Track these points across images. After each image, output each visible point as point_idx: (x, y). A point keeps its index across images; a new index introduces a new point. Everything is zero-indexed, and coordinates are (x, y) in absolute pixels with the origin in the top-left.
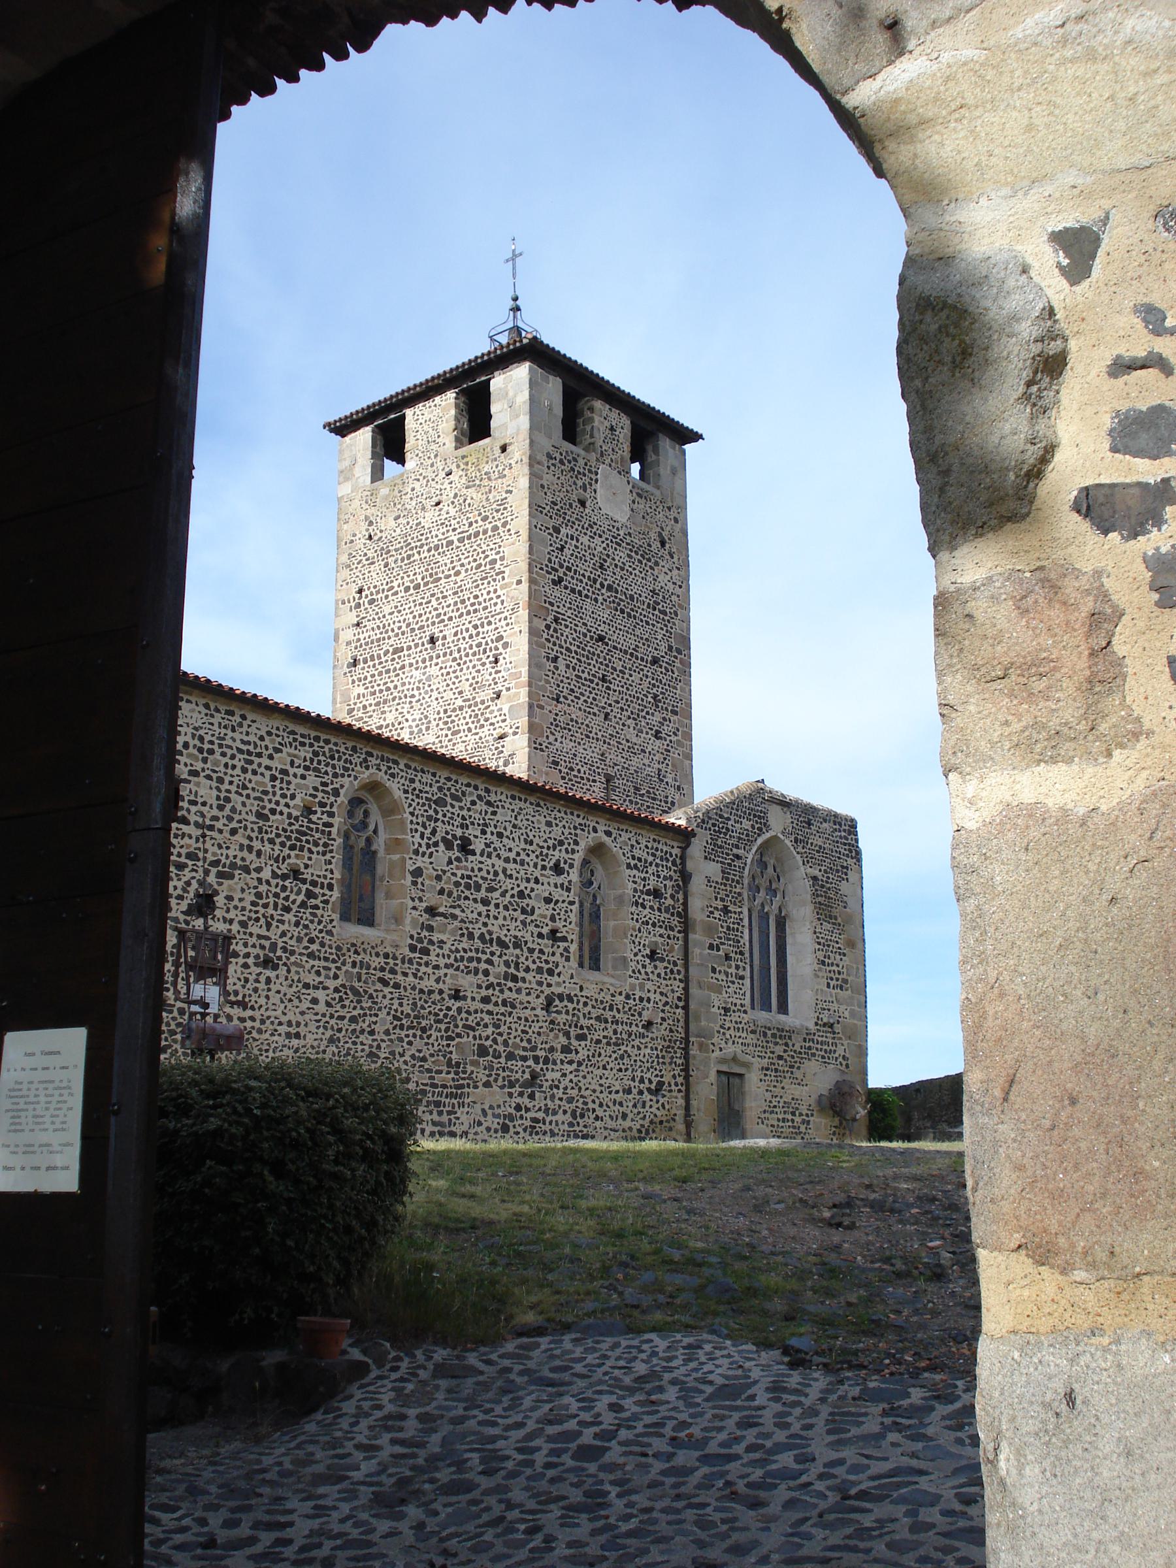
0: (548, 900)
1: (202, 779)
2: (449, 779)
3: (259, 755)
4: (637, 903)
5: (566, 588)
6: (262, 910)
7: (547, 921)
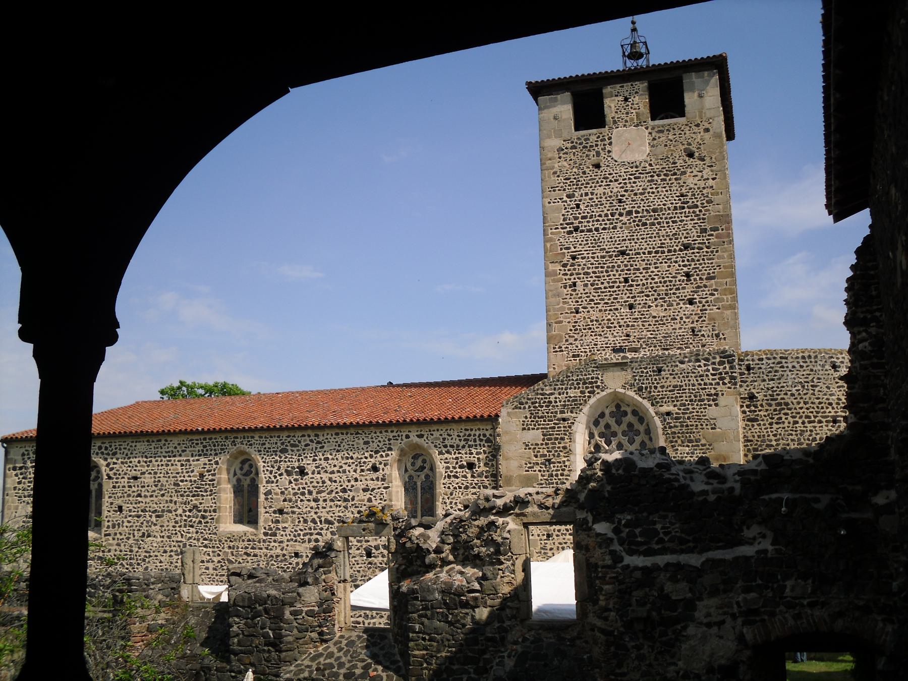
0: (365, 490)
1: (146, 475)
2: (289, 436)
3: (175, 456)
4: (449, 477)
5: (582, 231)
6: (178, 529)
7: (365, 502)
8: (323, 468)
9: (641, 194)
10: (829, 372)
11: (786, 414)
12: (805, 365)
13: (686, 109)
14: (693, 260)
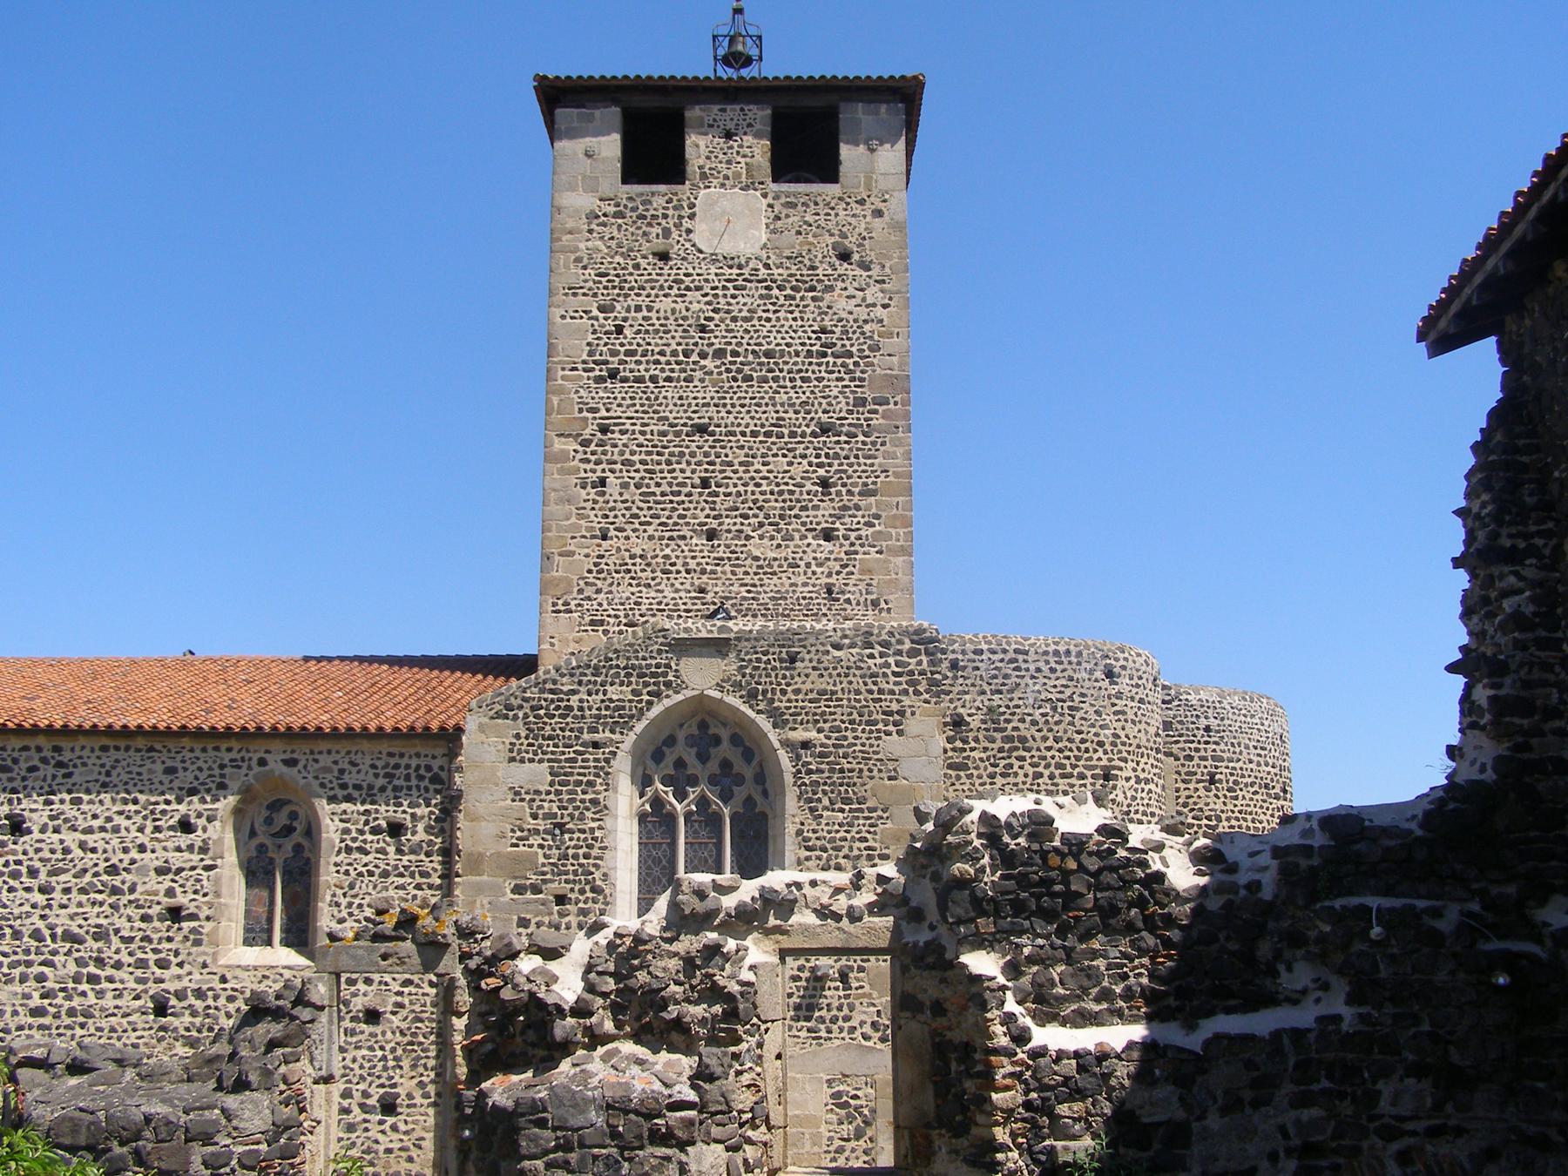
0: (161, 871)
4: (349, 850)
8: (66, 820)
9: (746, 319)
10: (1101, 684)
11: (1022, 759)
12: (1059, 667)
13: (842, 169)
14: (837, 456)
